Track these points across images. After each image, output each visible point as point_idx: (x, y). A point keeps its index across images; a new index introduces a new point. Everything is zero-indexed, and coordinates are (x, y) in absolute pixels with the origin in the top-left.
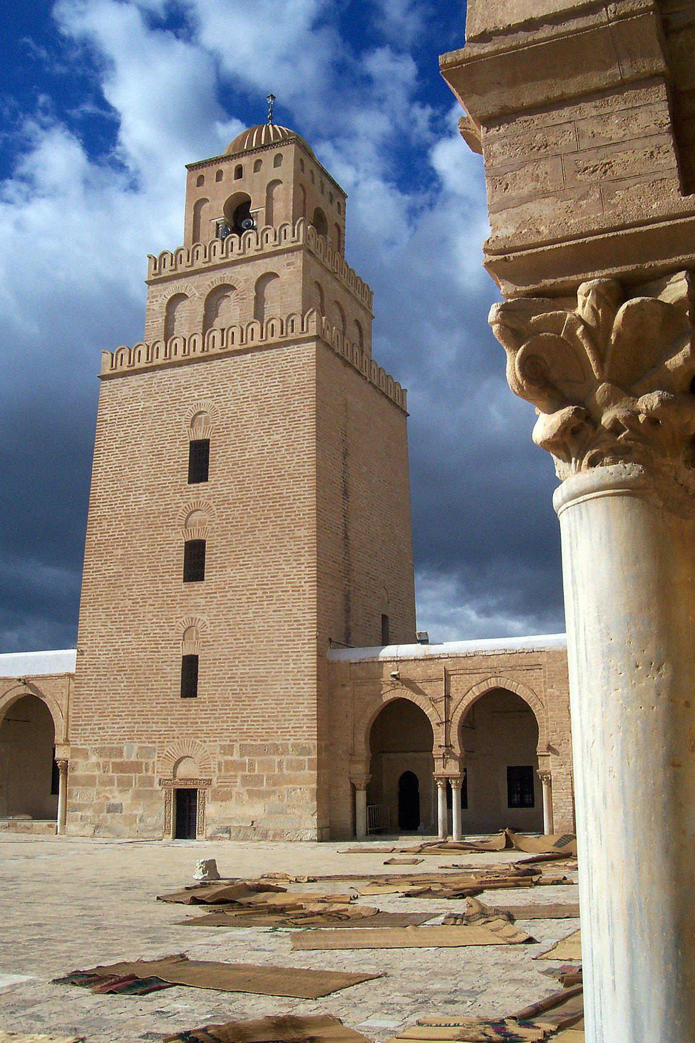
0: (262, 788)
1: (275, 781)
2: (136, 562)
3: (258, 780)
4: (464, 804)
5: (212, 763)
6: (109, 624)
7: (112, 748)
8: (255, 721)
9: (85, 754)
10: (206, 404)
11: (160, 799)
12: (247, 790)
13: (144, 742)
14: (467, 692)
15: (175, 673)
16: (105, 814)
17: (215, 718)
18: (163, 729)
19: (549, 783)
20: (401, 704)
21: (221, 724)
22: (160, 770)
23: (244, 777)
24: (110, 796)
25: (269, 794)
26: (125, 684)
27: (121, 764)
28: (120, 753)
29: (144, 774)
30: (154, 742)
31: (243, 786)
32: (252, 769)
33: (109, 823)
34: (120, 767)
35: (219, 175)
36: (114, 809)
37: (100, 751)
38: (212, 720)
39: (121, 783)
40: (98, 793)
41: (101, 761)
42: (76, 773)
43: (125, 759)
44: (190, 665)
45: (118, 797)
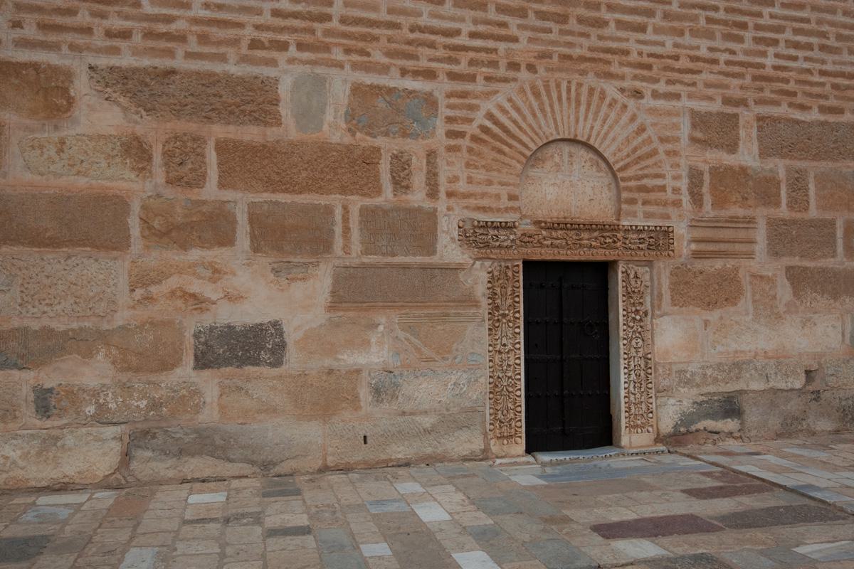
0: (829, 263)
5: (667, 169)
7: (210, 80)
8: (797, 45)
12: (789, 269)
13: (385, 69)
16: (185, 371)
17: (666, 16)
18: (467, 27)
21: (687, 39)
23: (775, 226)
24: (209, 291)
27: (264, 152)
28: (256, 101)
29: (387, 196)
30: (430, 74)
32: (799, 201)
33: (209, 416)
36: (250, 346)
38: (657, 20)
40: (141, 280)
43: (289, 129)
45: (252, 292)
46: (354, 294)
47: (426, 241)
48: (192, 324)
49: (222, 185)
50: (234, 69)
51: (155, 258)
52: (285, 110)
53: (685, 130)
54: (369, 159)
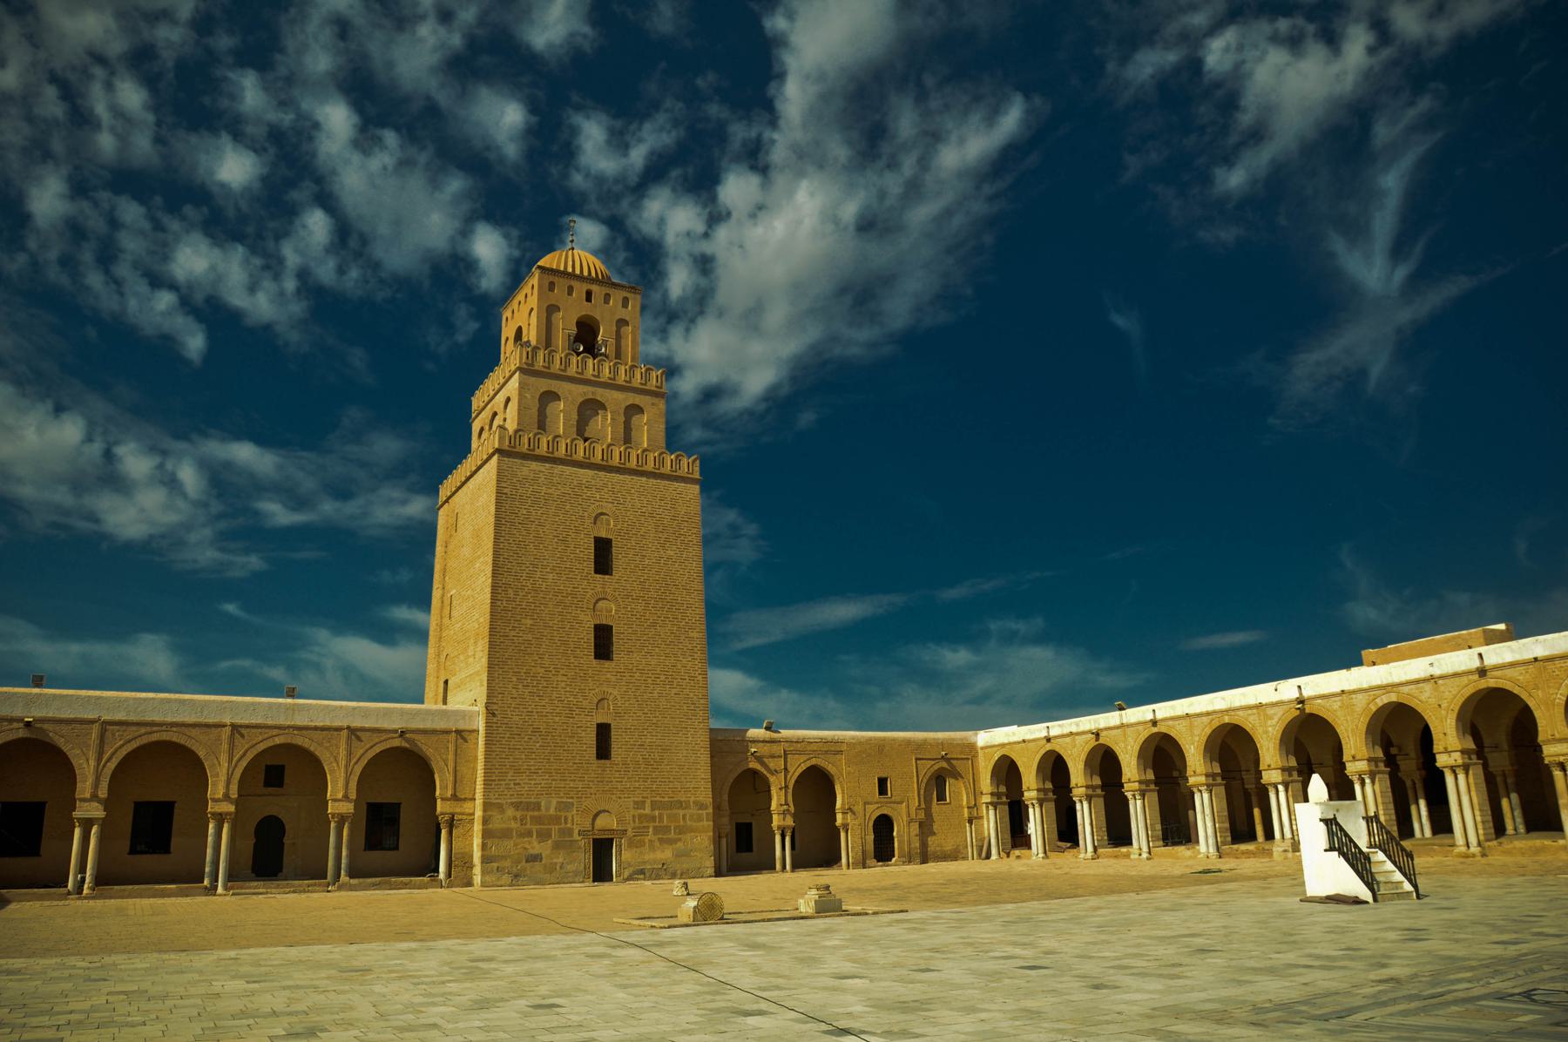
1: (681, 830)
3: (667, 829)
4: (793, 847)
9: (500, 808)
10: (608, 508)
14: (798, 766)
15: (591, 738)
20: (755, 772)
22: (578, 822)
25: (676, 841)
28: (537, 806)
34: (538, 820)
35: (570, 290)
36: (535, 858)
37: (517, 806)
39: (539, 834)
41: (518, 814)
44: (603, 731)
45: (535, 847)
46: (557, 846)
47: (571, 835)
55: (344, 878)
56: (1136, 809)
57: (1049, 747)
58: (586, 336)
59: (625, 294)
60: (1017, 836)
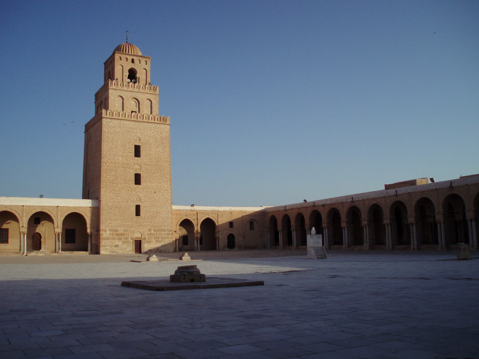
1: (163, 238)
2: (119, 177)
6: (112, 194)
11: (131, 243)
15: (134, 210)
16: (113, 247)
19: (219, 240)
23: (154, 237)
26: (118, 211)
28: (117, 230)
29: (125, 236)
30: (128, 228)
31: (154, 239)
32: (157, 235)
34: (116, 235)
36: (117, 246)
37: (110, 230)
39: (119, 239)
41: (110, 232)
42: (102, 236)
43: (119, 232)
44: (138, 208)
47: (128, 239)
48: (114, 245)
49: (115, 236)
50: (116, 228)
51: (112, 241)
52: (119, 231)
53: (147, 230)
54: (124, 234)
55: (60, 251)
56: (345, 233)
57: (285, 213)
58: (132, 75)
59: (145, 59)
60: (275, 241)
